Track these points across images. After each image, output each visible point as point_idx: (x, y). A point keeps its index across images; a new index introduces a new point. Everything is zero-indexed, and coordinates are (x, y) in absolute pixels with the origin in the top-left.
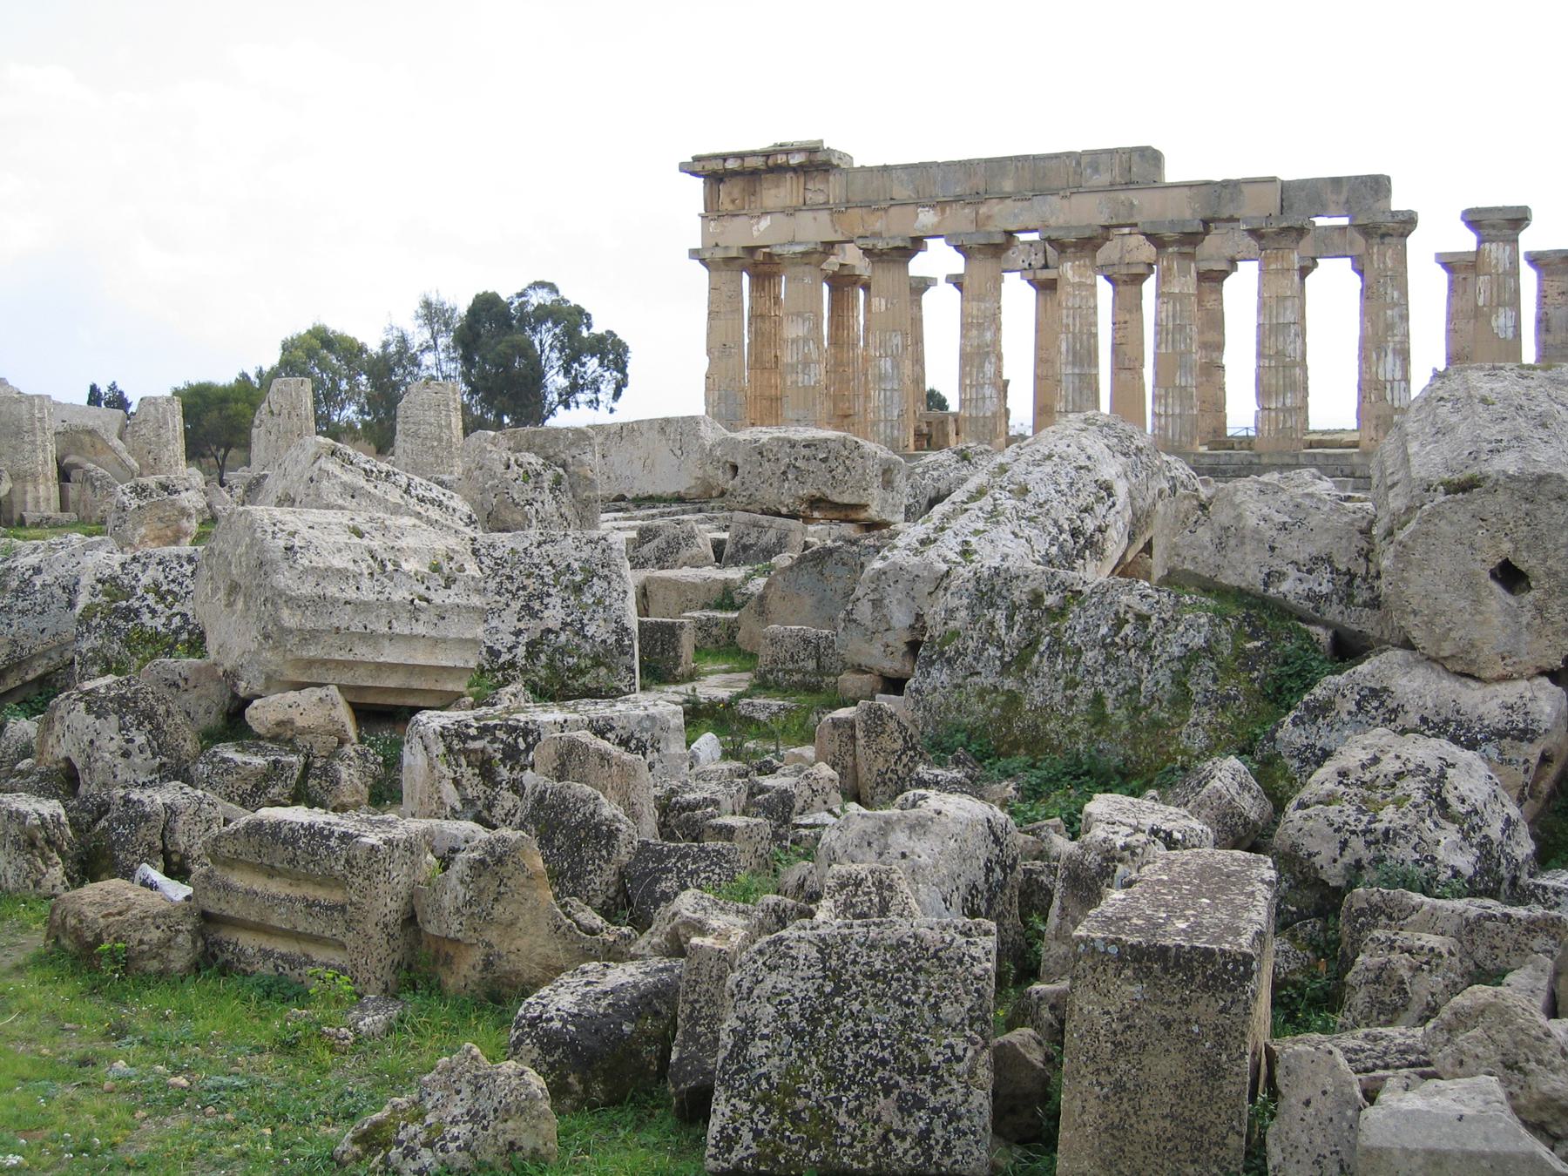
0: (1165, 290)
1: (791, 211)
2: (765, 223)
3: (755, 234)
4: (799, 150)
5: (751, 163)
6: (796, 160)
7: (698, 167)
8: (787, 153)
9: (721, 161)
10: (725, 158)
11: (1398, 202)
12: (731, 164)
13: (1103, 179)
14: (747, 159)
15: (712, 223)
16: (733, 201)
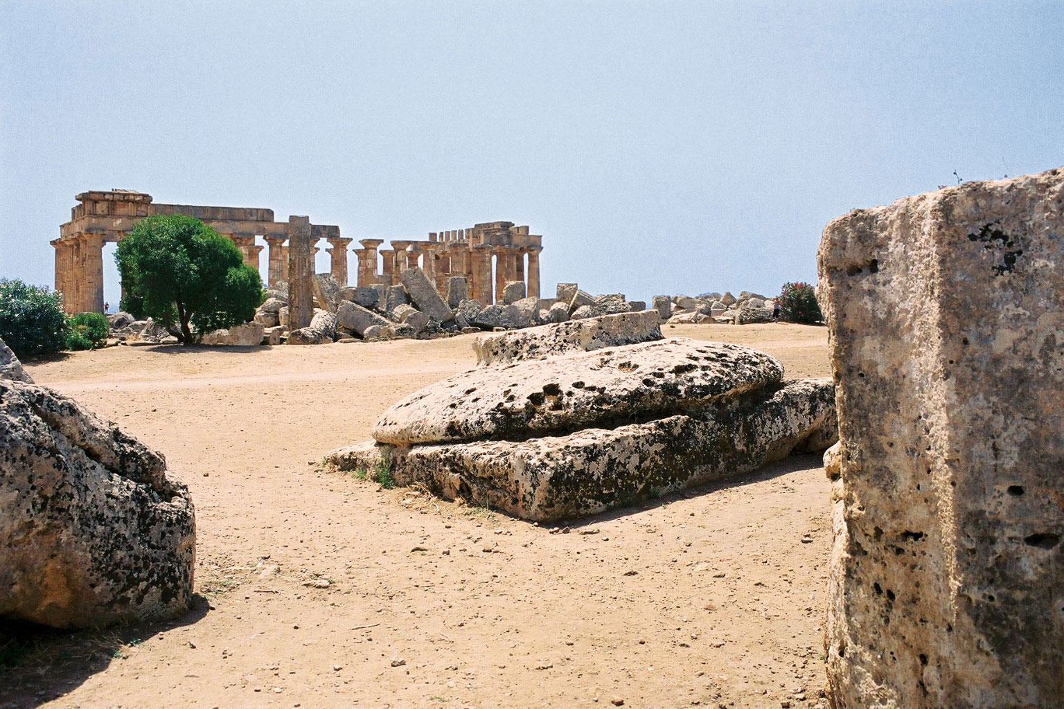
0: (276, 258)
1: (130, 217)
2: (119, 221)
3: (114, 225)
4: (140, 195)
5: (116, 197)
6: (137, 199)
7: (92, 197)
8: (134, 195)
9: (102, 195)
10: (104, 194)
11: (343, 235)
12: (107, 197)
13: (255, 218)
14: (115, 196)
15: (94, 220)
16: (103, 211)
